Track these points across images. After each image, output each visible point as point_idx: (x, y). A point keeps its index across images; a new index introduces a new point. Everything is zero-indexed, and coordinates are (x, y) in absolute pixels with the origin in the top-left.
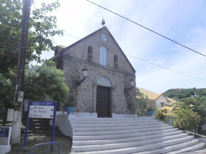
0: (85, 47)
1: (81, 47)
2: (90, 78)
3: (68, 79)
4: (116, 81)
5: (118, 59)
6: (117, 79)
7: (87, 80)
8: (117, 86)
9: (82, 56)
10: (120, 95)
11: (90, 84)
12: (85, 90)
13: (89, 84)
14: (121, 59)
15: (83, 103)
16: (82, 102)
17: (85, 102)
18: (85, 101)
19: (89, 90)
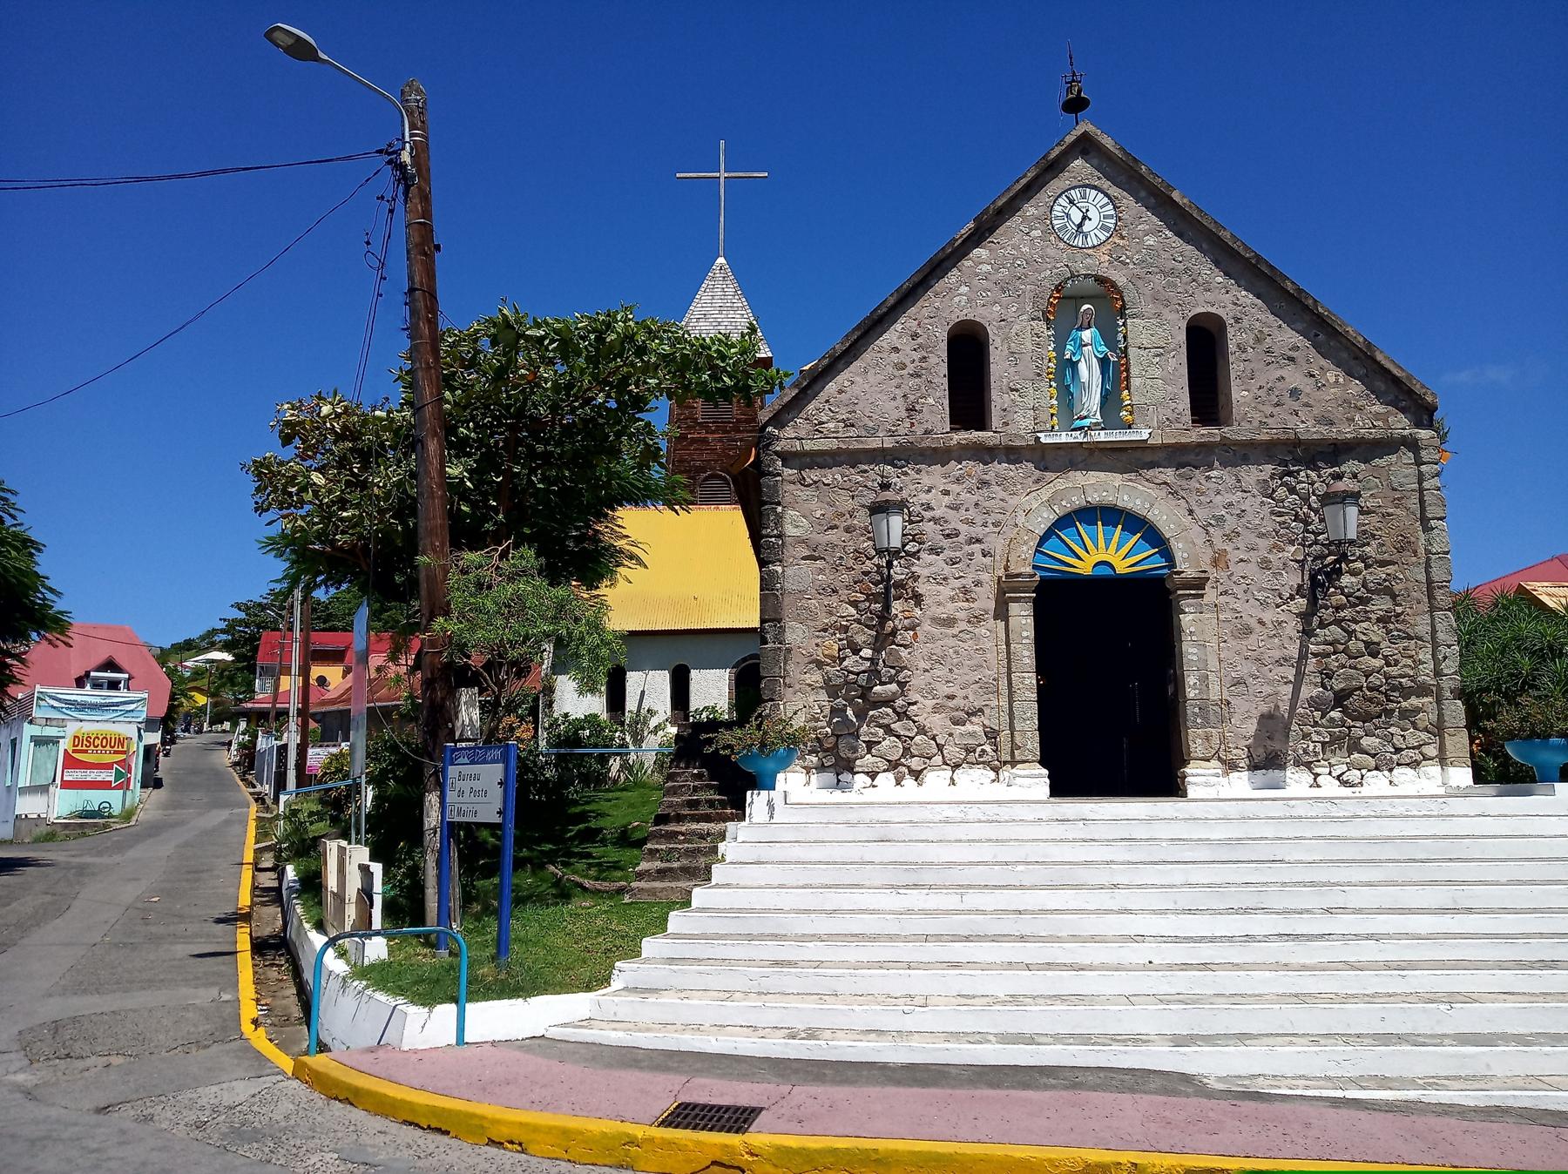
0: (920, 340)
1: (896, 350)
2: (979, 541)
3: (820, 577)
4: (1220, 519)
5: (1232, 347)
6: (1231, 504)
7: (958, 554)
8: (1233, 556)
9: (911, 410)
10: (1261, 622)
11: (985, 577)
12: (949, 622)
13: (978, 583)
14: (1258, 340)
15: (937, 709)
16: (930, 703)
17: (951, 704)
18: (951, 697)
19: (976, 619)
